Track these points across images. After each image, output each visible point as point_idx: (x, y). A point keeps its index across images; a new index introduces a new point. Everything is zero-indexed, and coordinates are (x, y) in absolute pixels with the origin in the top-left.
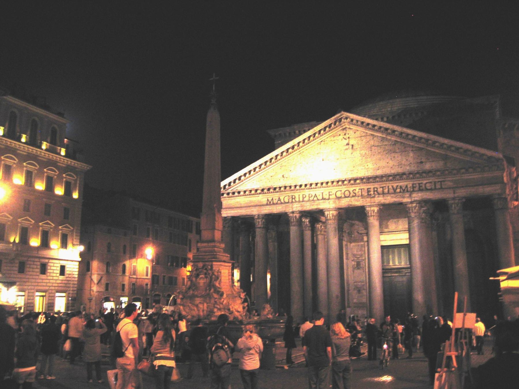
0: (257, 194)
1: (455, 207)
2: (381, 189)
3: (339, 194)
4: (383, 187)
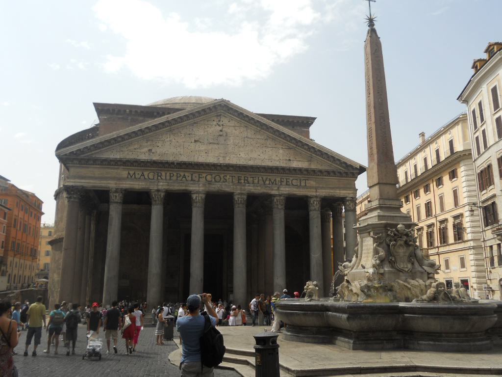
0: (118, 165)
1: (316, 204)
2: (252, 179)
3: (209, 178)
4: (253, 178)
